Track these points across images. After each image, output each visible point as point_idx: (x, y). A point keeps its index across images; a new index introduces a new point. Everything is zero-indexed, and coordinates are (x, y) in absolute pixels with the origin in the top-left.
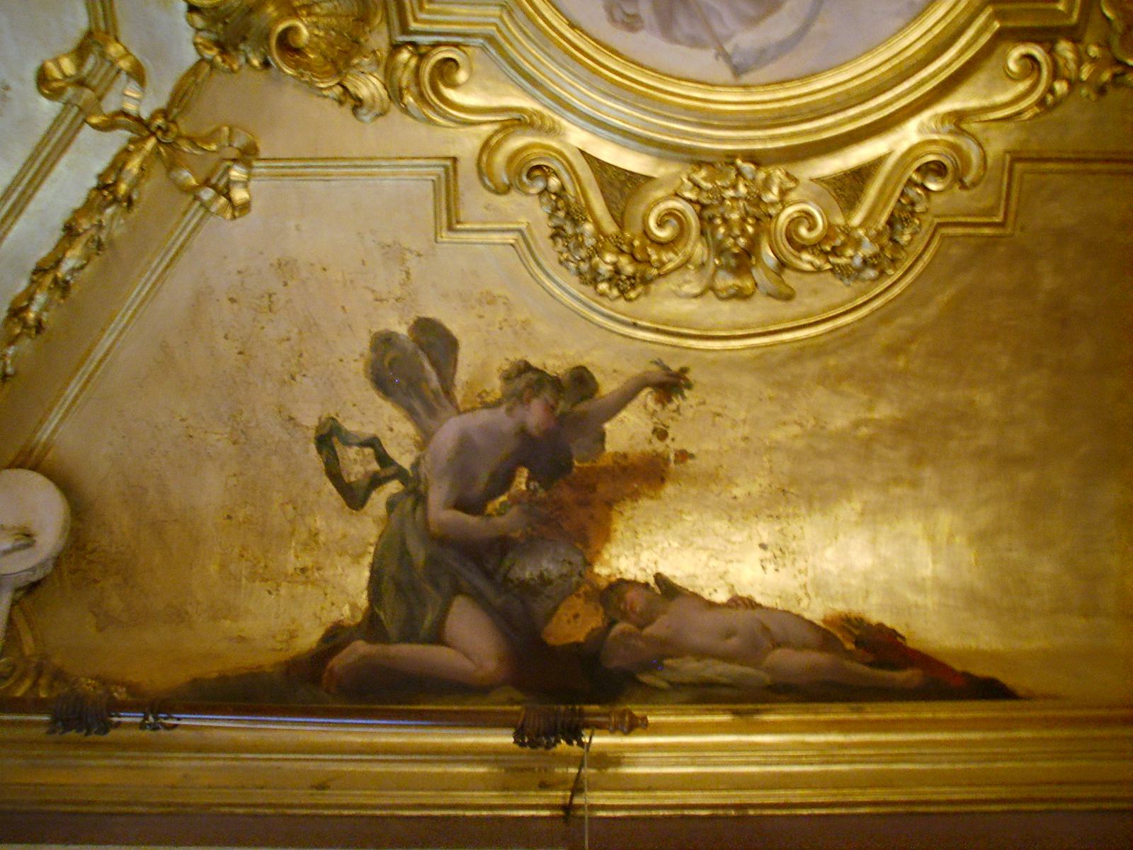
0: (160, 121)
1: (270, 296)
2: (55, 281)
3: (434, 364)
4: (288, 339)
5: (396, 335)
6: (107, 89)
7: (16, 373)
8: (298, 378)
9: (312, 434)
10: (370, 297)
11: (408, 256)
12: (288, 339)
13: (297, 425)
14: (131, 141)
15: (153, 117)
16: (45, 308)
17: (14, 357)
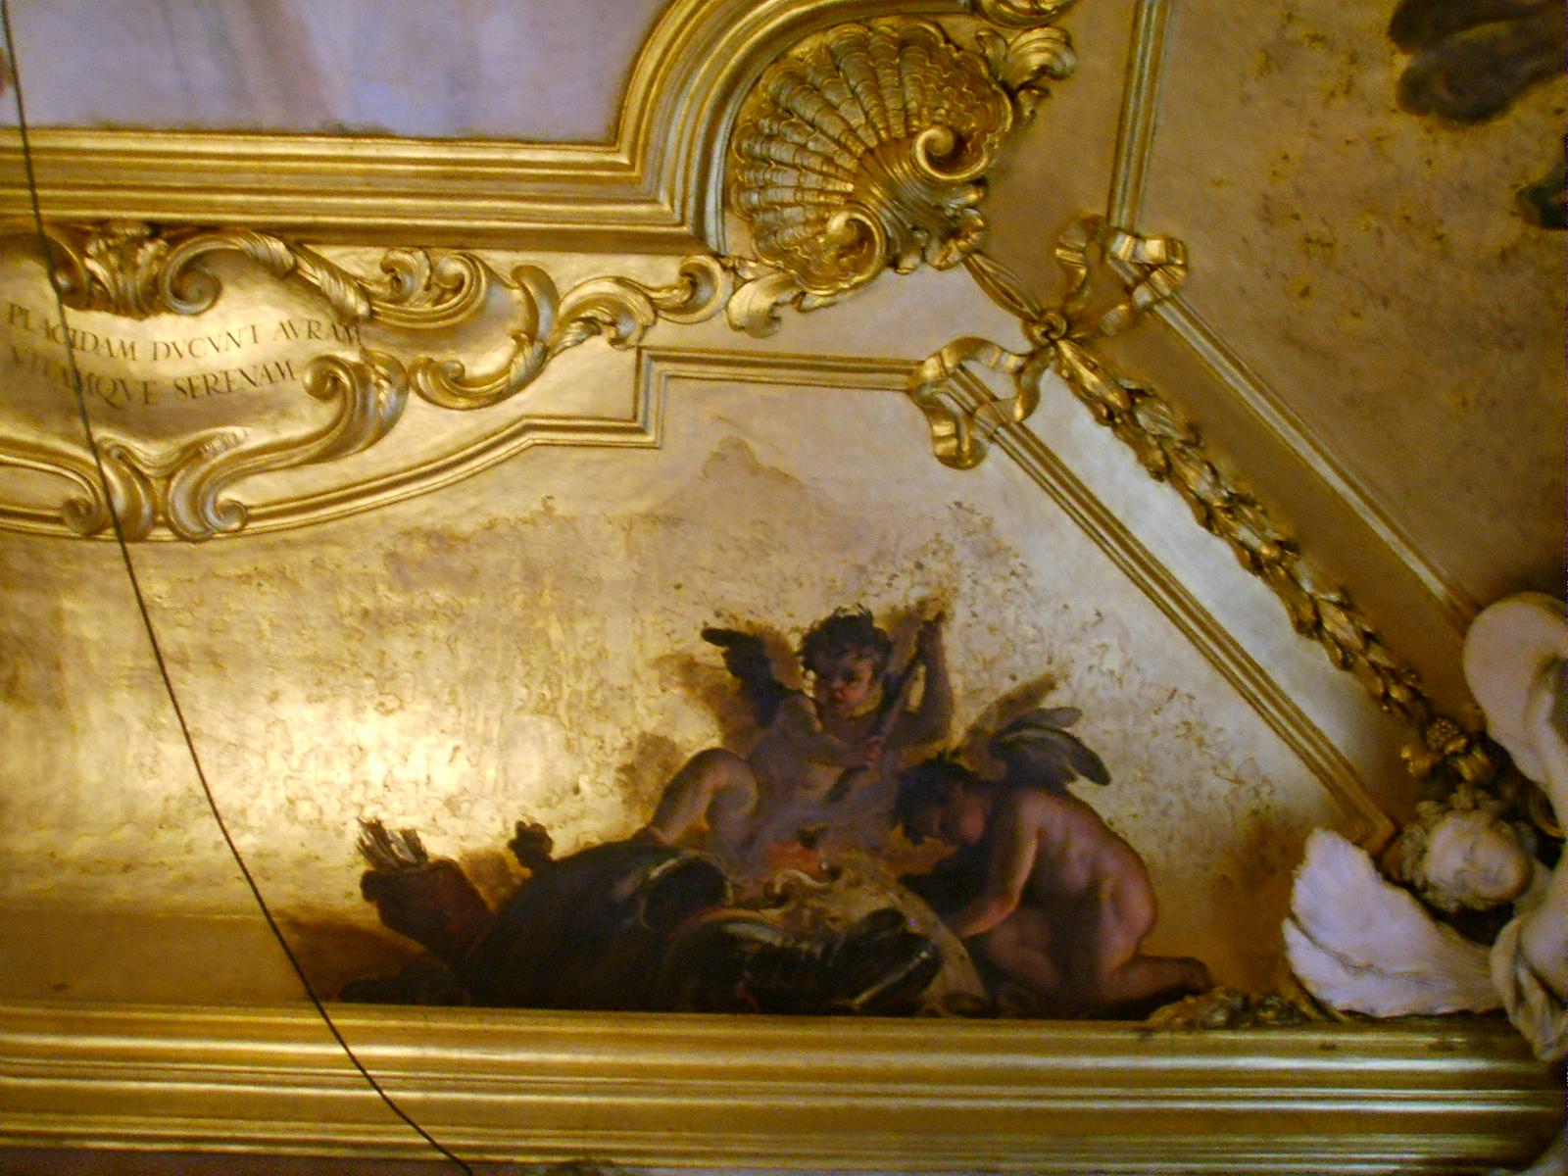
0: (1037, 331)
1: (1309, 241)
2: (1228, 510)
3: (1469, 23)
4: (1380, 232)
5: (1408, 71)
6: (983, 388)
7: (1342, 590)
8: (1440, 231)
9: (1534, 232)
10: (1340, 102)
11: (1289, 34)
12: (1380, 232)
13: (1515, 249)
14: (1058, 371)
15: (1031, 337)
16: (1258, 529)
17: (1315, 585)
